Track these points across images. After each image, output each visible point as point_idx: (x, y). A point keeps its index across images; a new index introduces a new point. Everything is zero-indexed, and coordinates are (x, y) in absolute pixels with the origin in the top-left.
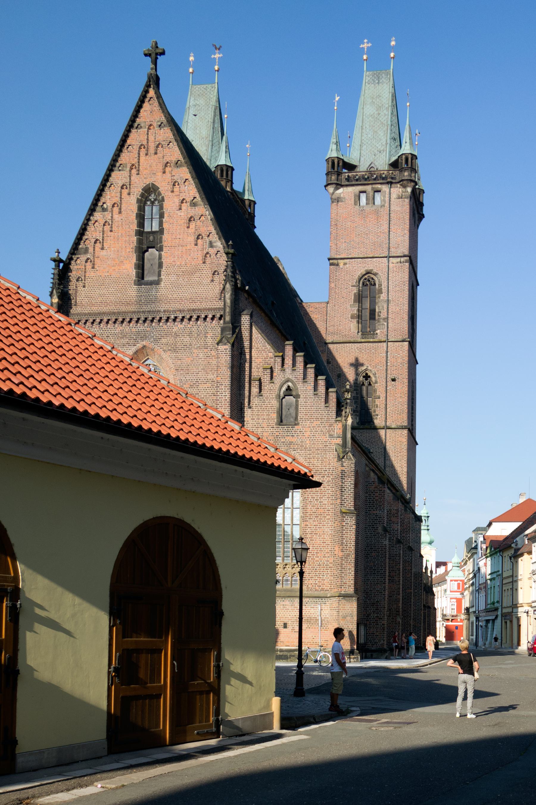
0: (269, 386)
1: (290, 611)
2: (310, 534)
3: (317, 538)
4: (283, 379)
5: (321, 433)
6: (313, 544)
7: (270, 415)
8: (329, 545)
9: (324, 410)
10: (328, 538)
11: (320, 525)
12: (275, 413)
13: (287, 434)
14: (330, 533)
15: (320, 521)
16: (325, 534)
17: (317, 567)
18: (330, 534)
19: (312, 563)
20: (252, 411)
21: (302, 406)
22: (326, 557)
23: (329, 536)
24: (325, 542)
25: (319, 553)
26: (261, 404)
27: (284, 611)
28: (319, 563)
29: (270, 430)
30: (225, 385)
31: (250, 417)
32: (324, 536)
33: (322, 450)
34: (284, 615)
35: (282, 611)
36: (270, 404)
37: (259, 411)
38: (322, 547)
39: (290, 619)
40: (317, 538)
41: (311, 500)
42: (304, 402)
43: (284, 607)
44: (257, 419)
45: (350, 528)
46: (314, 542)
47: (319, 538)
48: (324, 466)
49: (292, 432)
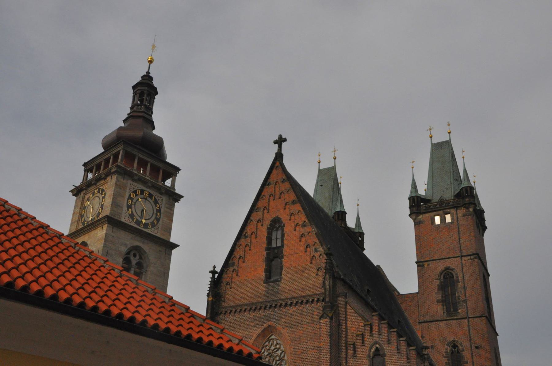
0: (361, 348)
36: (362, 363)
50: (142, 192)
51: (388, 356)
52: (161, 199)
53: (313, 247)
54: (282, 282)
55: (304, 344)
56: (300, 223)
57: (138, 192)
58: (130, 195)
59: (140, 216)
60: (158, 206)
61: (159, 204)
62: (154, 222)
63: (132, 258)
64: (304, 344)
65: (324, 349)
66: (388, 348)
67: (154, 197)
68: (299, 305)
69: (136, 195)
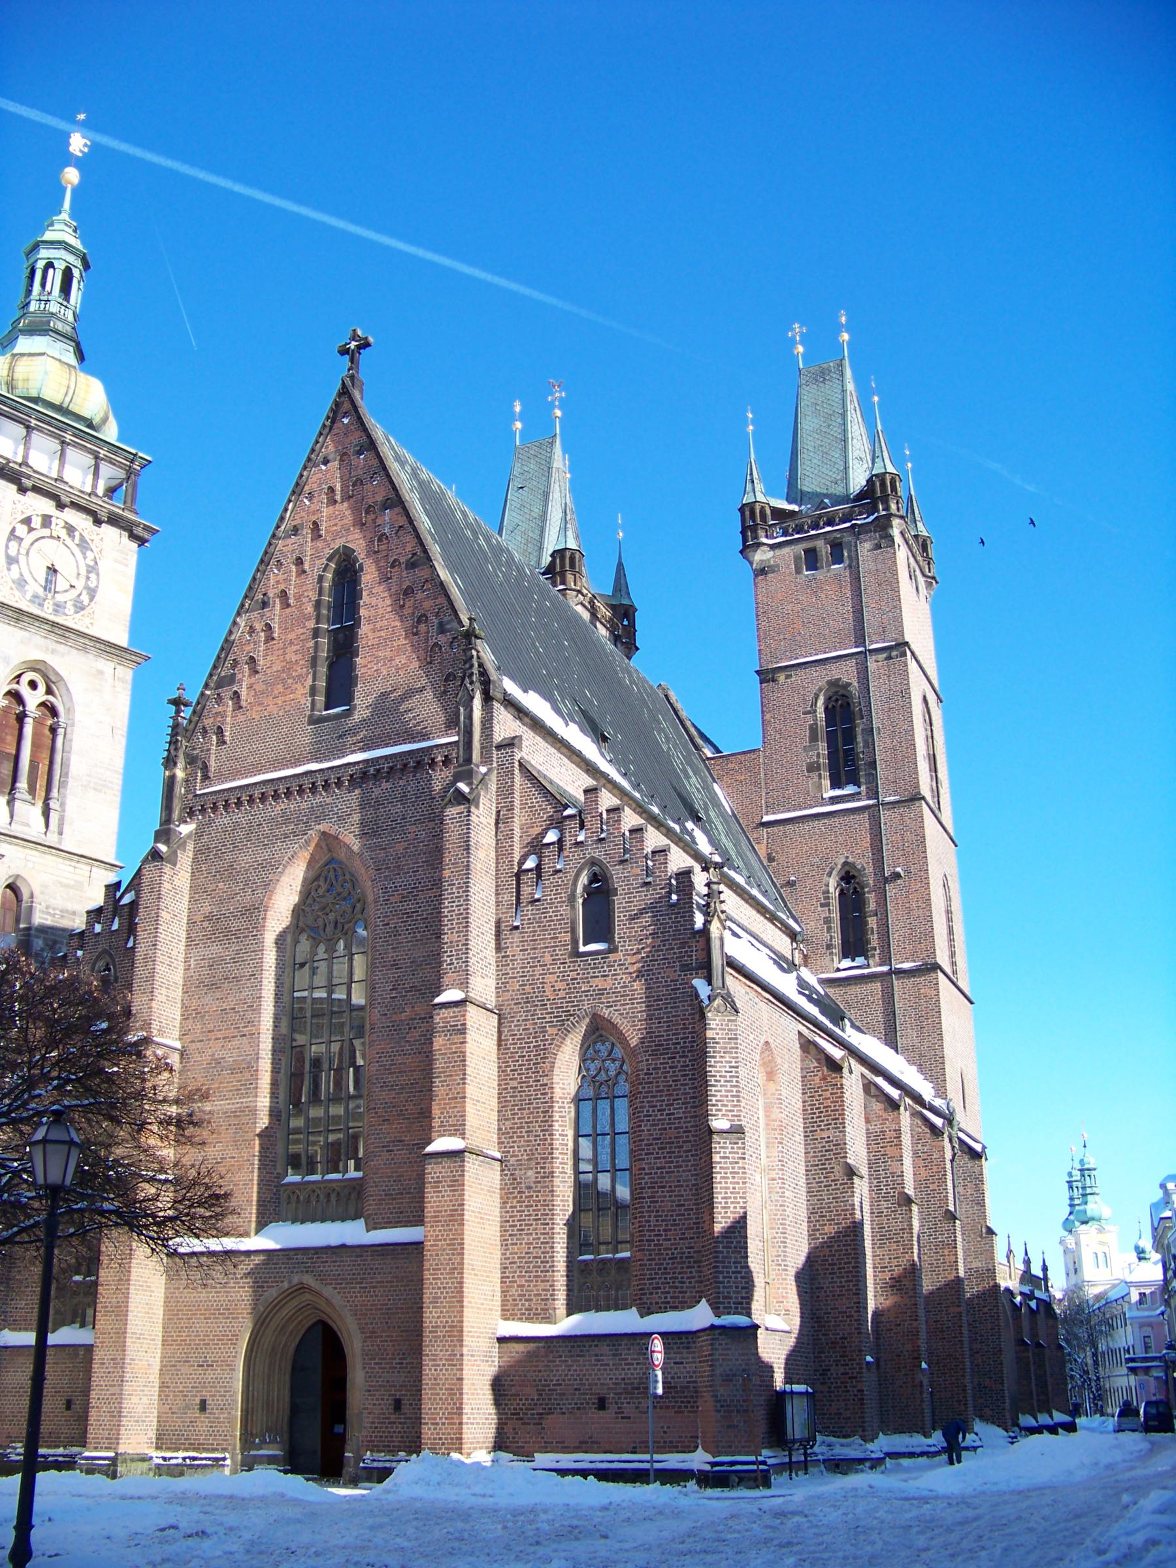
1: (611, 1370)
2: (649, 1188)
3: (665, 1197)
4: (583, 861)
5: (664, 964)
6: (657, 1211)
7: (557, 938)
8: (692, 1209)
9: (668, 915)
10: (688, 1195)
11: (670, 1167)
12: (567, 932)
13: (594, 973)
14: (694, 1182)
15: (670, 1157)
16: (682, 1186)
17: (668, 1264)
18: (693, 1185)
19: (656, 1255)
20: (521, 933)
21: (623, 912)
22: (687, 1238)
23: (691, 1190)
24: (684, 1205)
25: (670, 1230)
26: (540, 918)
27: (599, 1370)
28: (673, 1254)
29: (559, 968)
30: (459, 883)
31: (518, 946)
32: (679, 1191)
33: (667, 999)
34: (599, 1379)
35: (594, 1370)
36: (556, 916)
37: (536, 931)
38: (677, 1215)
39: (611, 1388)
40: (665, 1197)
41: (648, 1111)
42: (626, 902)
43: (599, 1361)
44: (531, 949)
45: (733, 1168)
46: (660, 1207)
47: (670, 1196)
48: (673, 1034)
49: (602, 967)
50: (47, 521)
51: (621, 894)
52: (100, 537)
53: (436, 621)
54: (356, 717)
55: (410, 877)
56: (403, 560)
57: (36, 522)
58: (13, 530)
59: (43, 584)
60: (93, 558)
61: (92, 550)
62: (81, 597)
63: (25, 690)
64: (410, 877)
65: (454, 884)
66: (623, 873)
67: (81, 534)
68: (398, 775)
69: (31, 530)
